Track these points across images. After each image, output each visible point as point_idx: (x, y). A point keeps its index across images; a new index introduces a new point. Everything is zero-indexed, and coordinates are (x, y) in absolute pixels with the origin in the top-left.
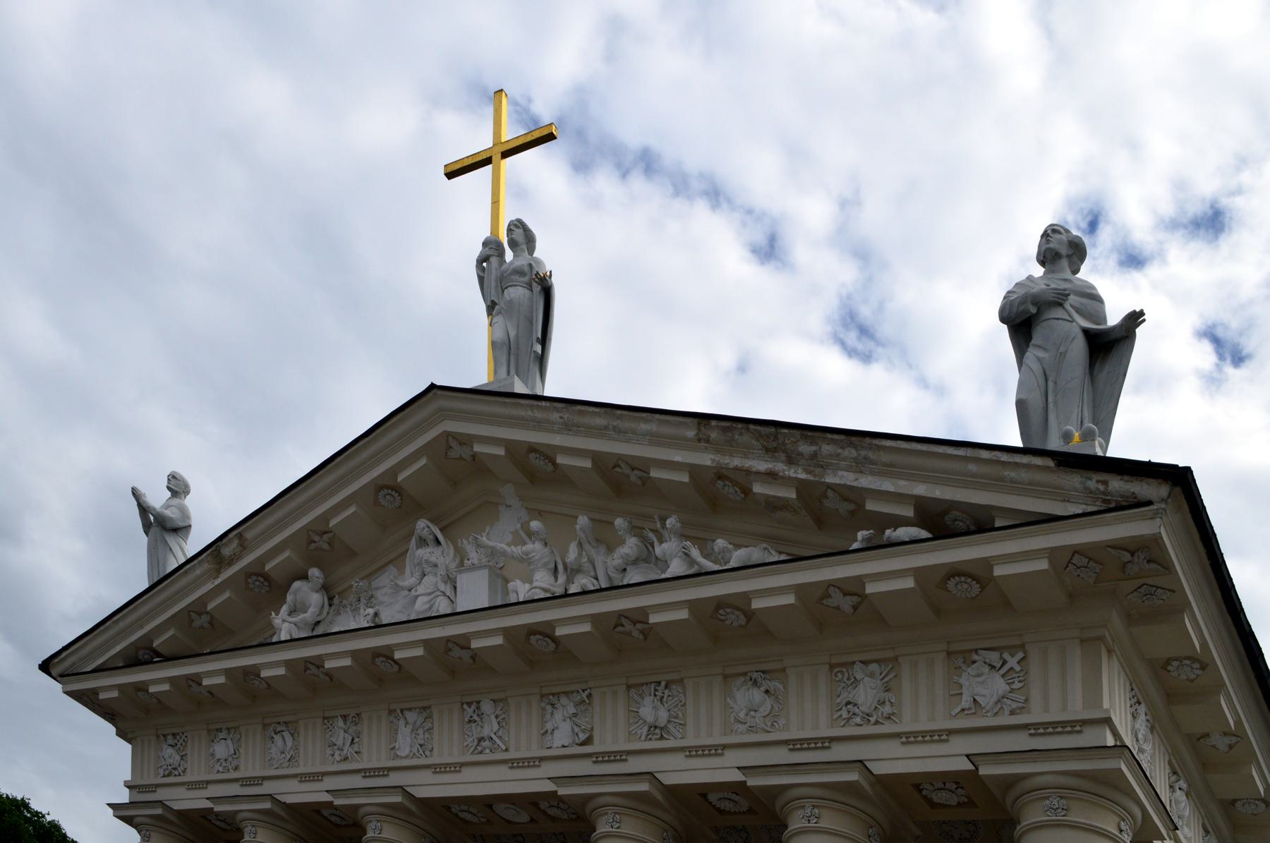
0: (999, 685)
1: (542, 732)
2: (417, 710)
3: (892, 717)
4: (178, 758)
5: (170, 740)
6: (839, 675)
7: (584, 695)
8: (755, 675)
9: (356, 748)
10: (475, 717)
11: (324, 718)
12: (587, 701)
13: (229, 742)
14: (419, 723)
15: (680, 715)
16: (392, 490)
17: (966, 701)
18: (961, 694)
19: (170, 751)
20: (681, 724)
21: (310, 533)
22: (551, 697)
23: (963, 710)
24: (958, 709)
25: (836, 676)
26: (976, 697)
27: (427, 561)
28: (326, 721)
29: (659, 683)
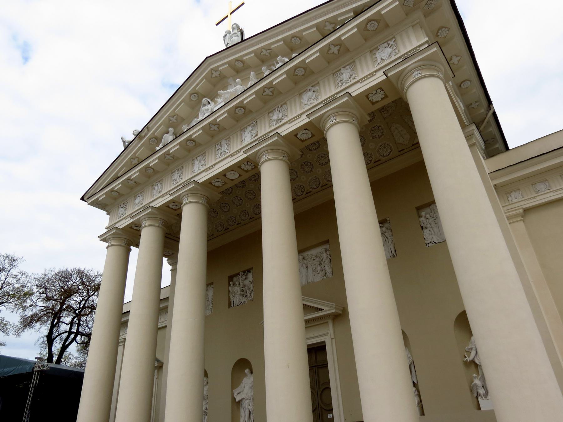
0: (389, 50)
1: (241, 141)
7: (255, 123)
9: (181, 177)
10: (220, 147)
11: (171, 173)
12: (256, 124)
13: (141, 197)
14: (201, 159)
15: (286, 113)
16: (195, 94)
17: (379, 60)
18: (377, 60)
20: (286, 115)
21: (170, 117)
23: (379, 64)
24: (377, 64)
25: (335, 75)
26: (383, 58)
28: (172, 174)
29: (279, 107)
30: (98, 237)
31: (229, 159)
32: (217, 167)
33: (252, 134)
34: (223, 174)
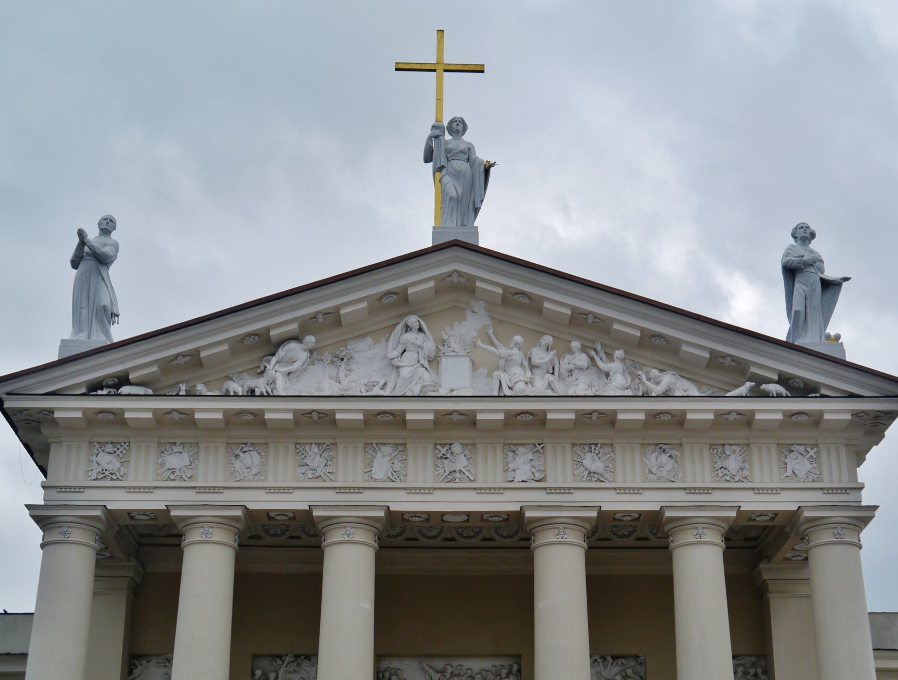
0: (808, 466)
2: (391, 445)
3: (747, 477)
4: (118, 465)
5: (109, 448)
6: (715, 451)
8: (664, 447)
12: (541, 452)
14: (394, 455)
15: (610, 465)
17: (789, 472)
19: (109, 458)
20: (611, 472)
22: (512, 446)
23: (787, 477)
24: (785, 476)
26: (794, 471)
27: (413, 344)
28: (298, 446)
29: (596, 445)
30: (28, 507)
31: (472, 495)
32: (438, 495)
33: (534, 470)
34: (443, 514)
